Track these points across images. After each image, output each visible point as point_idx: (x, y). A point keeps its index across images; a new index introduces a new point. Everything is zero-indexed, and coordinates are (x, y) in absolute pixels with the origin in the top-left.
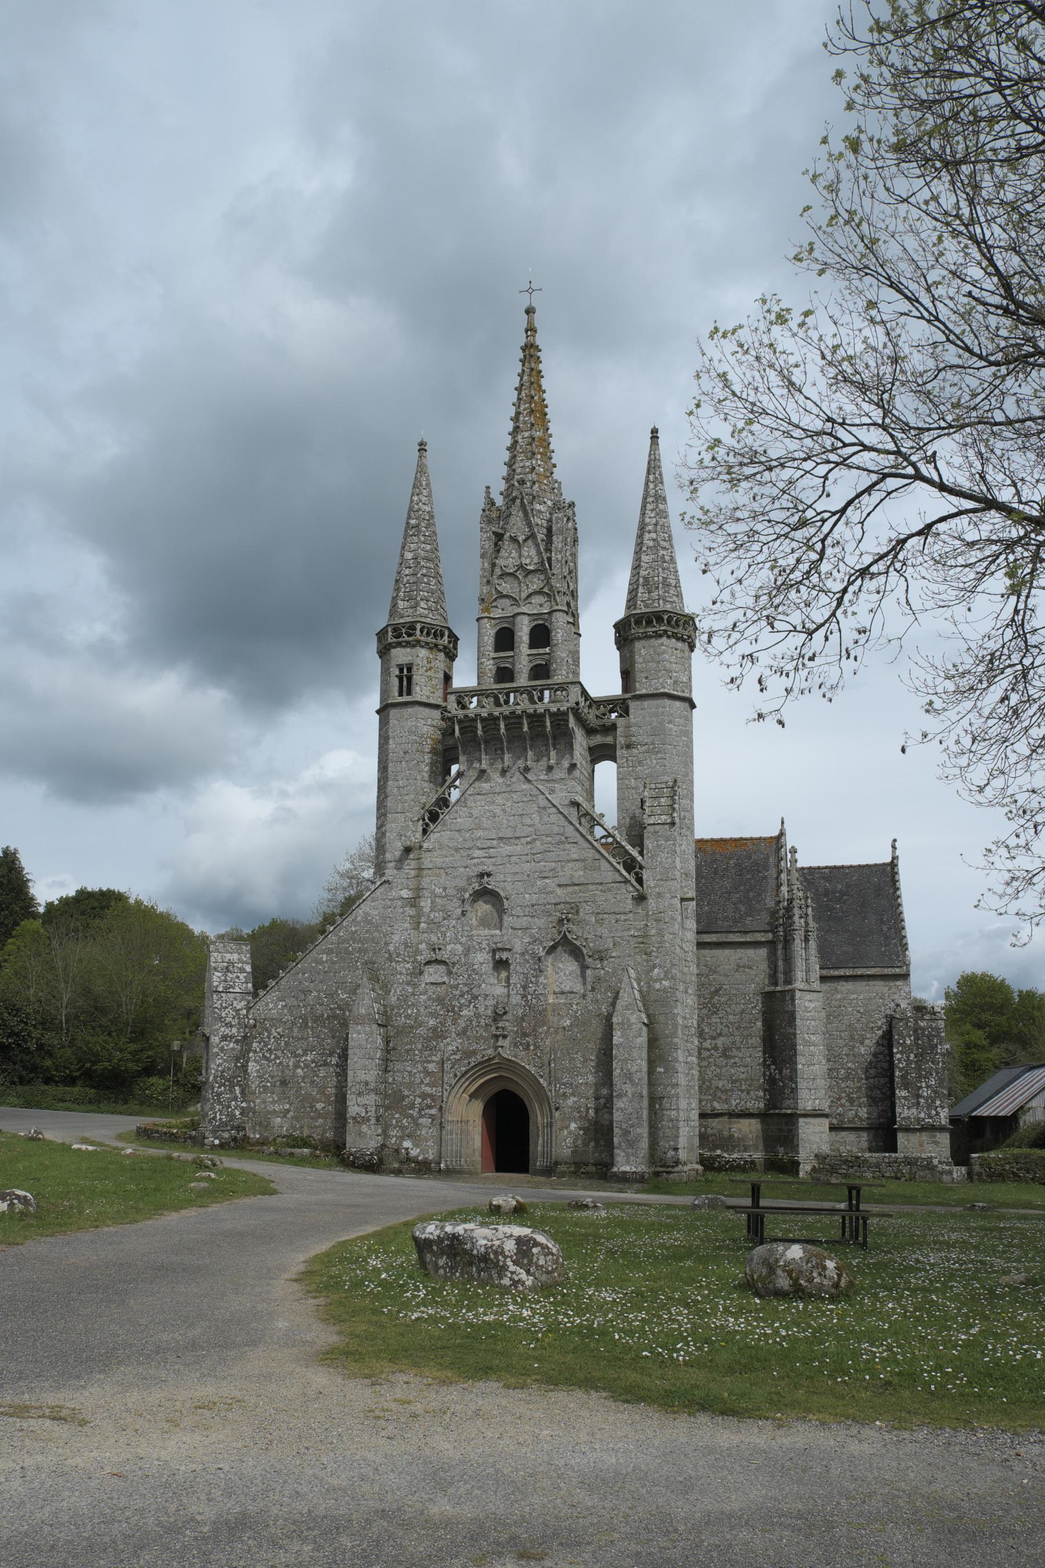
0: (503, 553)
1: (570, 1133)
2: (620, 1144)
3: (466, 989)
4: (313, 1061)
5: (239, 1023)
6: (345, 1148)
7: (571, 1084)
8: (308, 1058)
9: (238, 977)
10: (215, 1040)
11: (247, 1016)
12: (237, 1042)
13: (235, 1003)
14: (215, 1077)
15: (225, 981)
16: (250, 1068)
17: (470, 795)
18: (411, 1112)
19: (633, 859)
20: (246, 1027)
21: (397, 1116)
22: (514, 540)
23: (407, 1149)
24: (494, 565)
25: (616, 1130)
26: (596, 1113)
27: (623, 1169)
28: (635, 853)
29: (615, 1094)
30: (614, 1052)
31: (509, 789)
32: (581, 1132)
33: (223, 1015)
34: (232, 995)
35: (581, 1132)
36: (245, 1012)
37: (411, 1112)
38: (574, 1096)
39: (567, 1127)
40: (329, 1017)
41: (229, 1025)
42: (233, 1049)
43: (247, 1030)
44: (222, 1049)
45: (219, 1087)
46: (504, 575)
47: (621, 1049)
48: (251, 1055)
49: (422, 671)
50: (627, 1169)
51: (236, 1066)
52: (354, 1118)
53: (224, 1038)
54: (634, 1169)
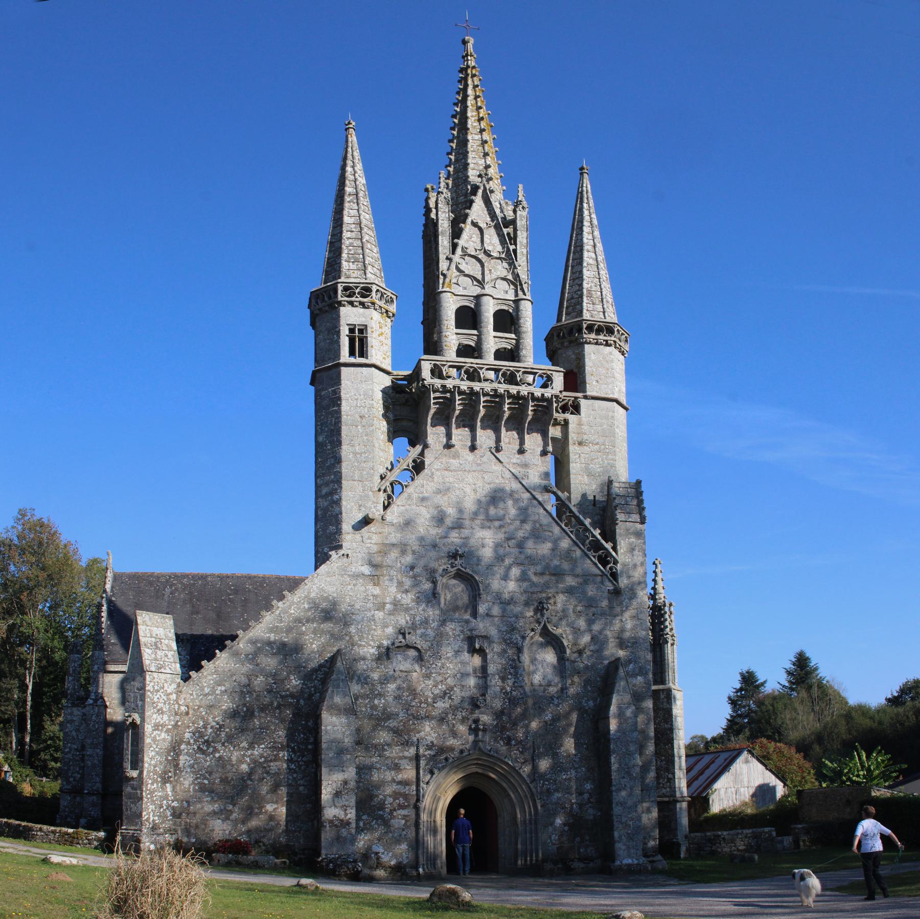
0: (465, 236)
1: (555, 829)
2: (620, 837)
3: (440, 678)
4: (261, 756)
5: (170, 711)
6: (319, 855)
7: (555, 781)
8: (256, 753)
9: (166, 656)
10: (148, 728)
11: (177, 701)
12: (168, 731)
13: (166, 685)
14: (149, 772)
15: (156, 659)
16: (181, 763)
17: (437, 470)
18: (381, 813)
19: (608, 554)
20: (176, 714)
21: (365, 817)
22: (475, 224)
23: (377, 853)
24: (454, 247)
25: (616, 824)
26: (580, 808)
27: (626, 861)
28: (608, 546)
29: (614, 788)
30: (612, 746)
31: (479, 468)
32: (566, 828)
33: (156, 700)
34: (162, 676)
35: (566, 828)
36: (174, 696)
37: (381, 813)
38: (558, 792)
39: (552, 824)
40: (279, 707)
41: (160, 712)
42: (164, 740)
43: (178, 718)
44: (154, 740)
45: (152, 784)
46: (465, 254)
47: (619, 744)
48: (183, 747)
49: (375, 335)
50: (630, 861)
51: (167, 759)
52: (331, 822)
53: (157, 727)
54: (636, 862)
